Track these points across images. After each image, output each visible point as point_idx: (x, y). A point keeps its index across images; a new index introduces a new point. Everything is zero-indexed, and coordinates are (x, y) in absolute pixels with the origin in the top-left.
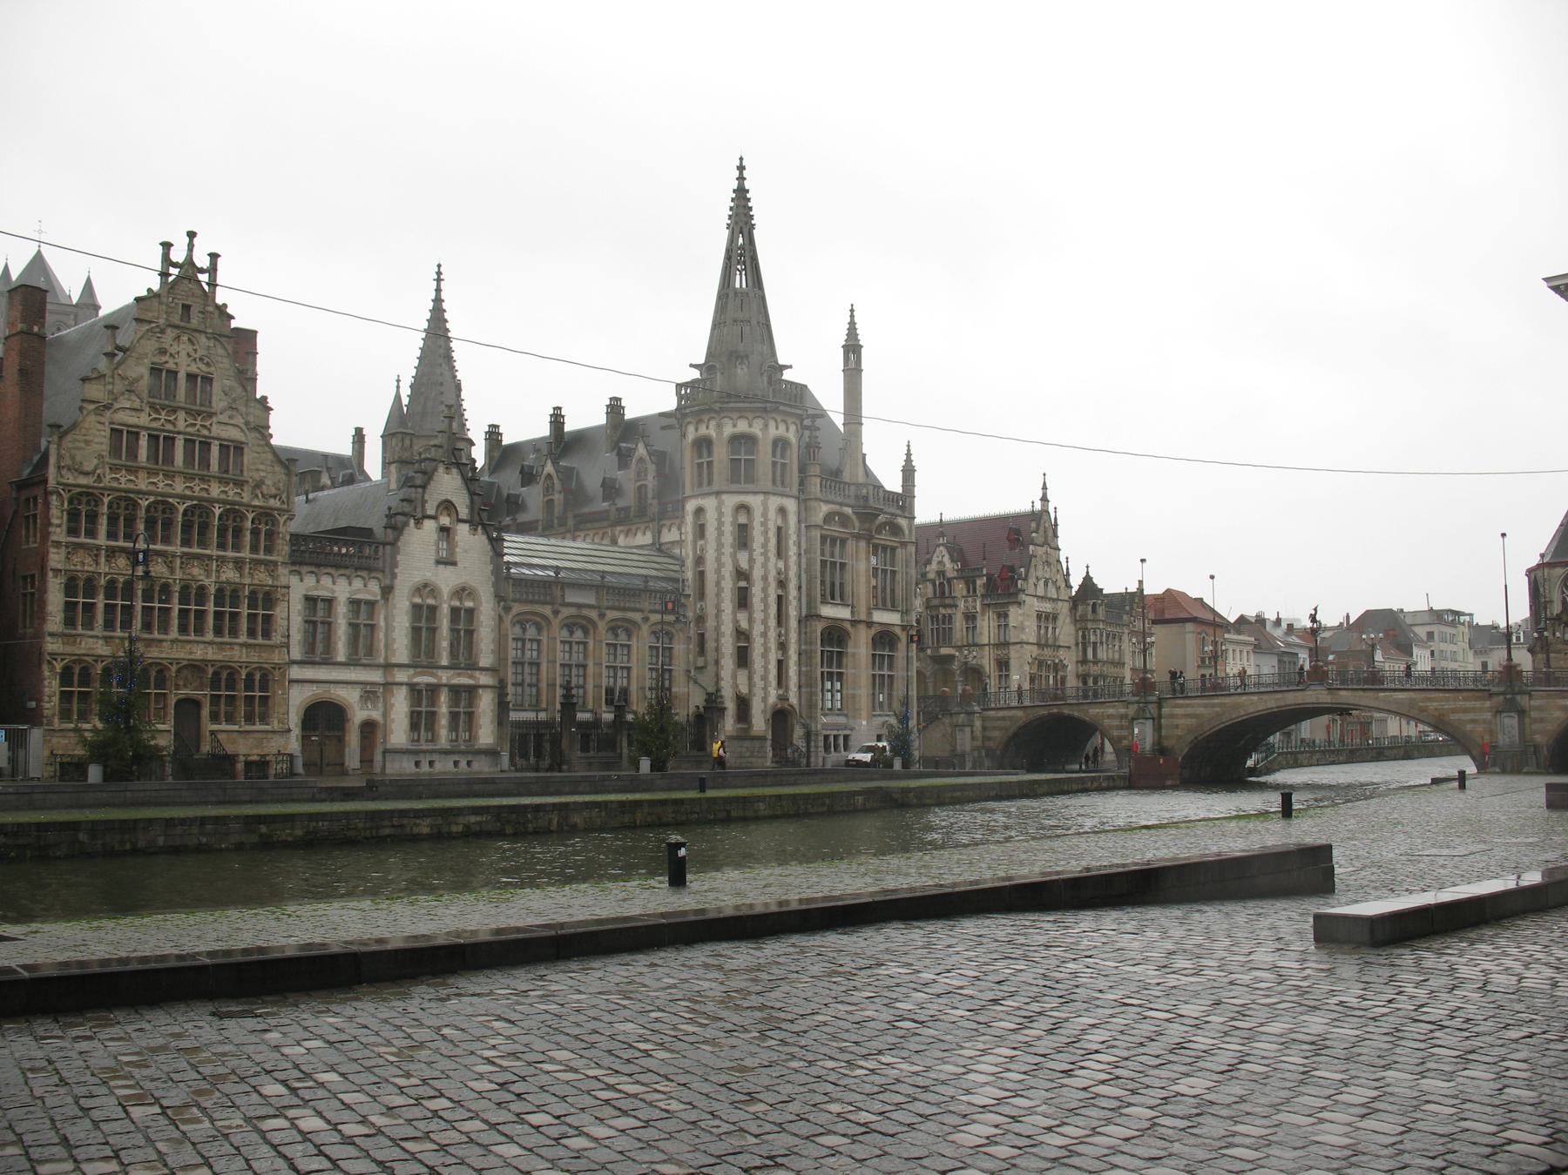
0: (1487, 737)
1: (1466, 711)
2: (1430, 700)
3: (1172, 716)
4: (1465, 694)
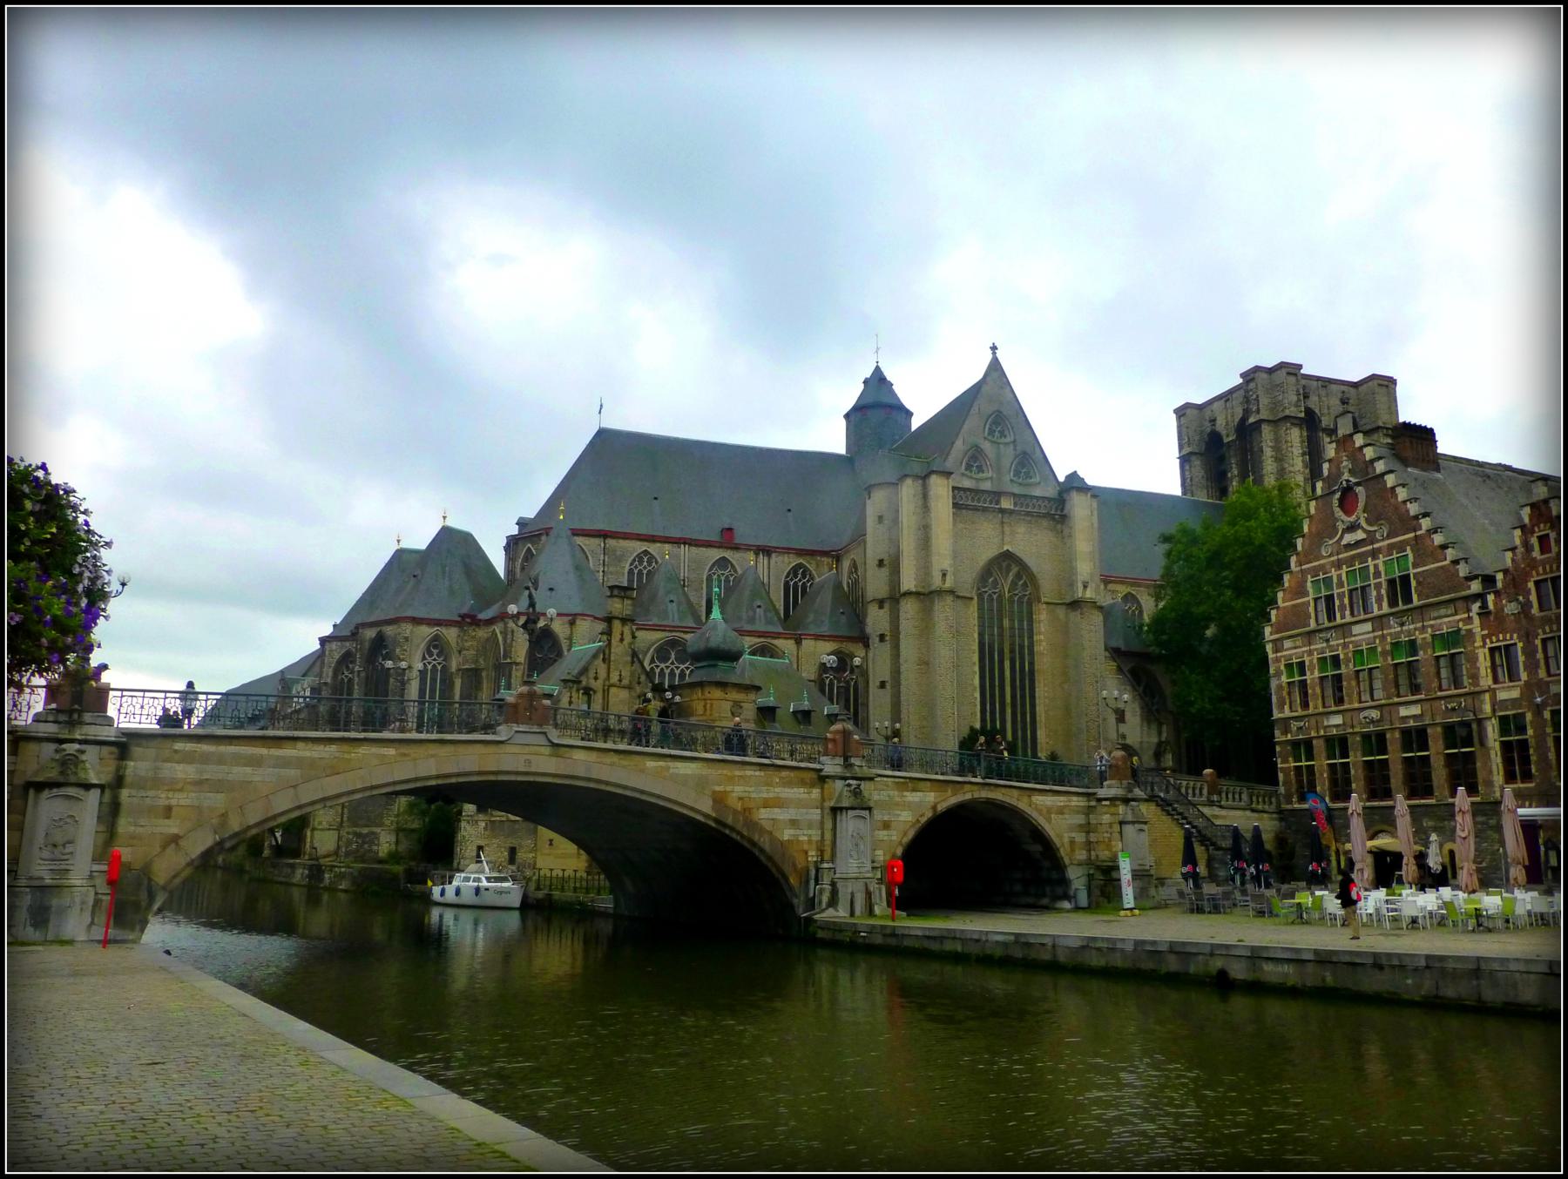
0: (813, 856)
1: (779, 803)
2: (731, 779)
3: (156, 782)
4: (784, 773)
